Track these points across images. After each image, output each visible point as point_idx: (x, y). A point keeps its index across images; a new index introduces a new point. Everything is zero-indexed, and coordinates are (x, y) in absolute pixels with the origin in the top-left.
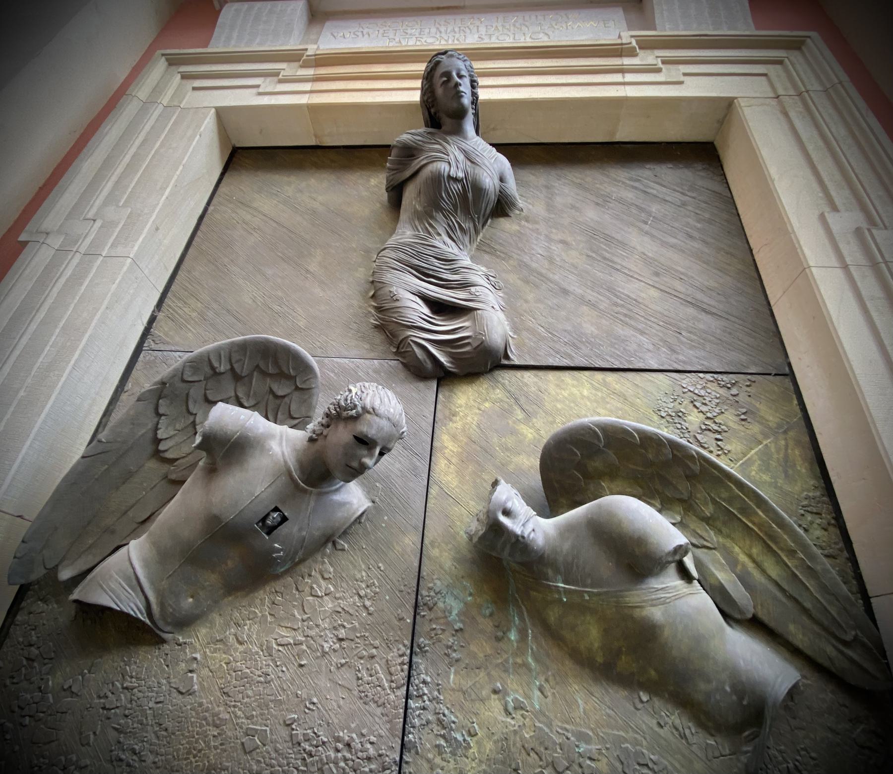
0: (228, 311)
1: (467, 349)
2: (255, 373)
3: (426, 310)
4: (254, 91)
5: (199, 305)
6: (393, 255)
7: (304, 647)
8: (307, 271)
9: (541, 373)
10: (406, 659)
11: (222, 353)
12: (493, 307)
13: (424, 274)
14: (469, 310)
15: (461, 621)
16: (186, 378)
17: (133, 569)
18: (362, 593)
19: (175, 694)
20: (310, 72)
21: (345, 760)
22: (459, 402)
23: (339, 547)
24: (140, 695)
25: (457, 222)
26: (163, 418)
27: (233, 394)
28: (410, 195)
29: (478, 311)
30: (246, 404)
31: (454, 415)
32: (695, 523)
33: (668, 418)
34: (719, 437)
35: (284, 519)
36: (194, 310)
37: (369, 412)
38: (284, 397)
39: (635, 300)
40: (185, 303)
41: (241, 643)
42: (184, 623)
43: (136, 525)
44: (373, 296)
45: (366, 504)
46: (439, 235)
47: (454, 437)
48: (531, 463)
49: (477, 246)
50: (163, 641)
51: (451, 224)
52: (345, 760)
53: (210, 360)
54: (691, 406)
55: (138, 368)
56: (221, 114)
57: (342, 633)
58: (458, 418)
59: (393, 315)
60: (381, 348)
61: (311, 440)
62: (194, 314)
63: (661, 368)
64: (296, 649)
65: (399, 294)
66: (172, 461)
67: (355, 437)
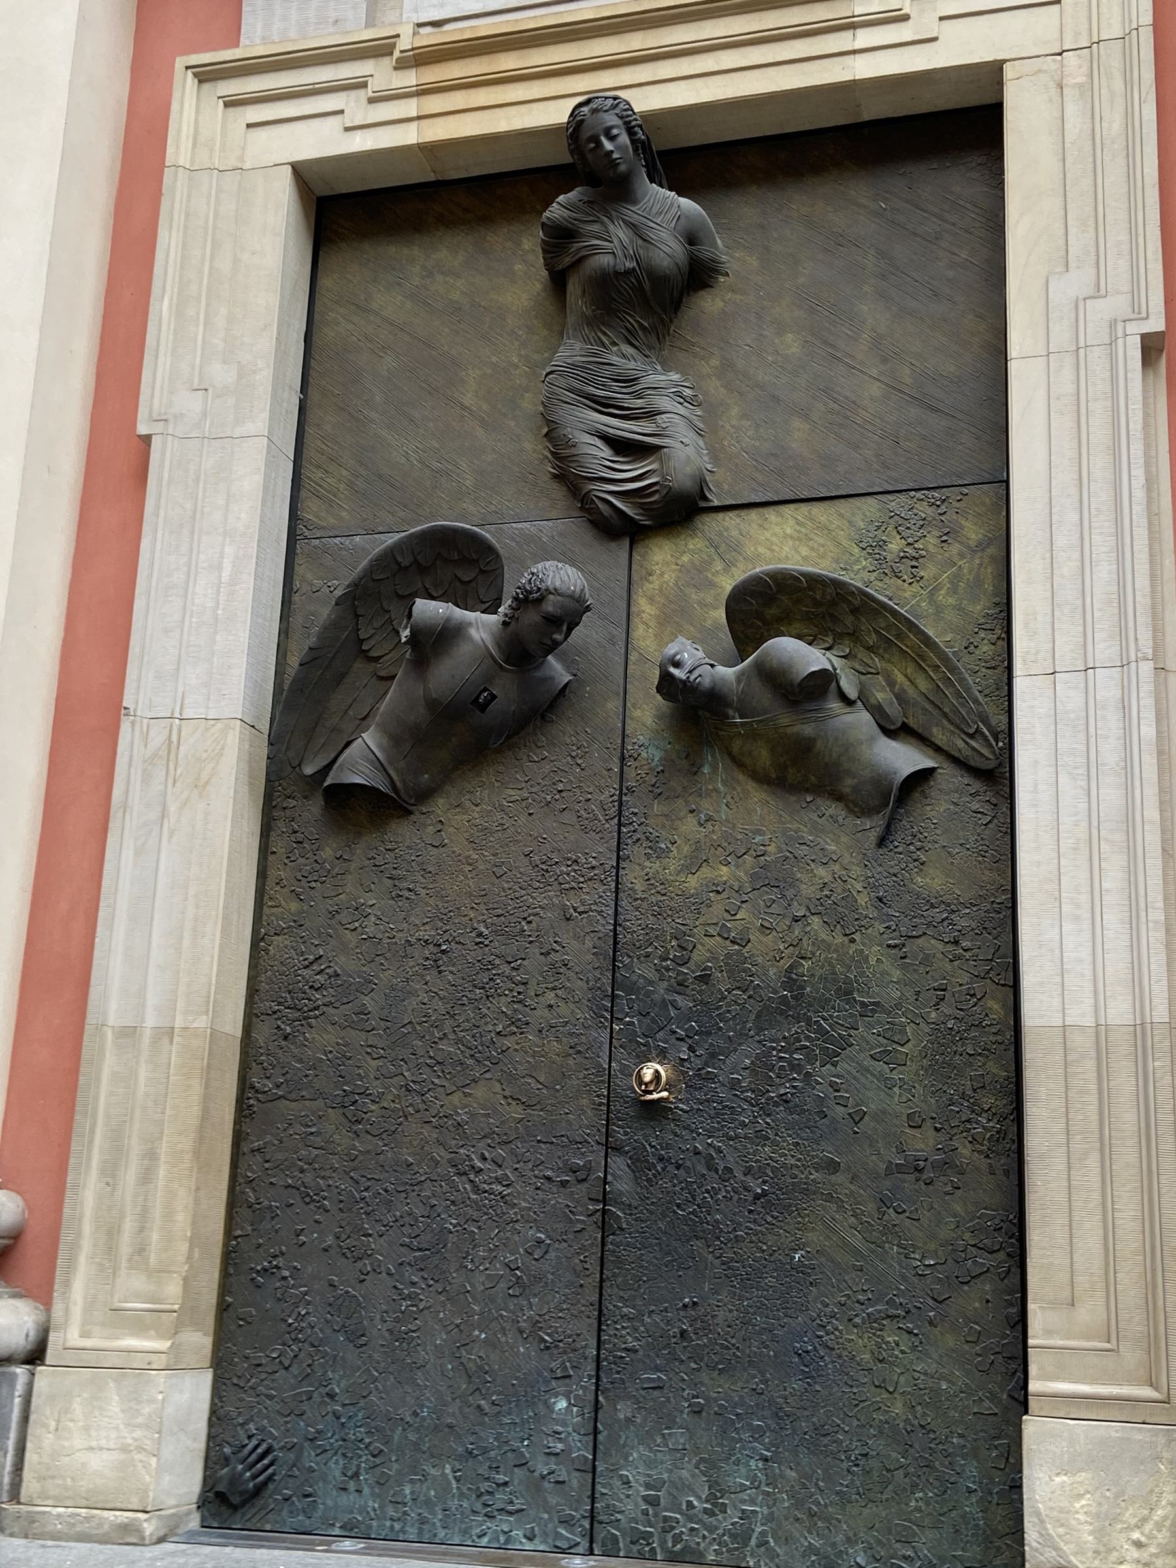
0: (380, 476)
1: (655, 498)
2: (438, 562)
3: (605, 452)
4: (334, 122)
5: (344, 472)
6: (562, 382)
7: (530, 801)
8: (463, 407)
9: (743, 513)
10: (615, 798)
11: (404, 547)
13: (602, 405)
14: (656, 449)
15: (662, 765)
17: (374, 754)
18: (574, 754)
19: (431, 848)
20: (410, 79)
21: (575, 871)
22: (656, 558)
24: (401, 853)
25: (637, 321)
27: (420, 585)
28: (573, 287)
29: (665, 450)
30: (435, 594)
31: (650, 575)
32: (862, 654)
33: (869, 550)
34: (914, 563)
35: (494, 697)
37: (553, 594)
38: (470, 582)
40: (326, 471)
41: (477, 805)
42: (425, 795)
43: (358, 722)
44: (546, 435)
45: (567, 678)
47: (651, 600)
48: (721, 615)
50: (411, 813)
51: (628, 325)
52: (575, 871)
54: (895, 533)
56: (302, 174)
57: (560, 786)
58: (655, 577)
59: (571, 465)
60: (564, 503)
61: (505, 623)
63: (871, 490)
64: (524, 804)
65: (574, 438)
66: (377, 659)
67: (544, 617)
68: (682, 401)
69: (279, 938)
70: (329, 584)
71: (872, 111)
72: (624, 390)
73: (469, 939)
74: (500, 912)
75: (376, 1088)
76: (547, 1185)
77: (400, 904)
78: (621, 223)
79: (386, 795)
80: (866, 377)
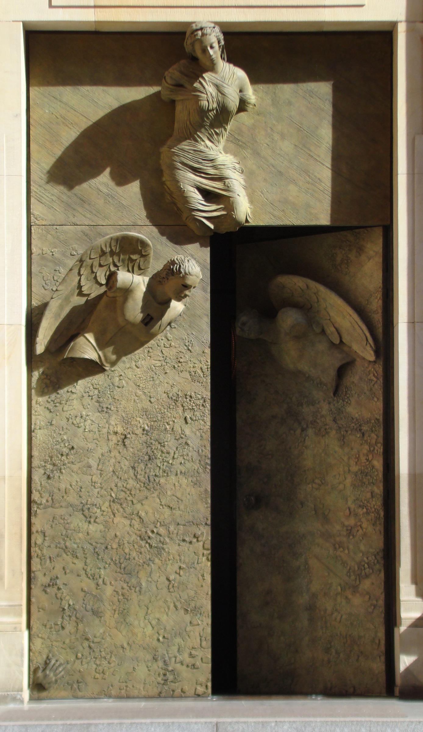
12: (238, 195)
13: (195, 170)
16: (92, 257)
23: (173, 327)
26: (82, 276)
36: (53, 195)
39: (319, 179)
41: (138, 367)
46: (203, 141)
49: (227, 137)
51: (210, 132)
53: (101, 248)
55: (35, 238)
62: (54, 198)
68: (235, 171)
69: (42, 431)
70: (53, 251)
71: (326, 29)
72: (207, 165)
73: (139, 431)
74: (154, 419)
75: (99, 501)
76: (184, 544)
77: (103, 415)
78: (211, 84)
79: (97, 362)
80: (325, 167)
